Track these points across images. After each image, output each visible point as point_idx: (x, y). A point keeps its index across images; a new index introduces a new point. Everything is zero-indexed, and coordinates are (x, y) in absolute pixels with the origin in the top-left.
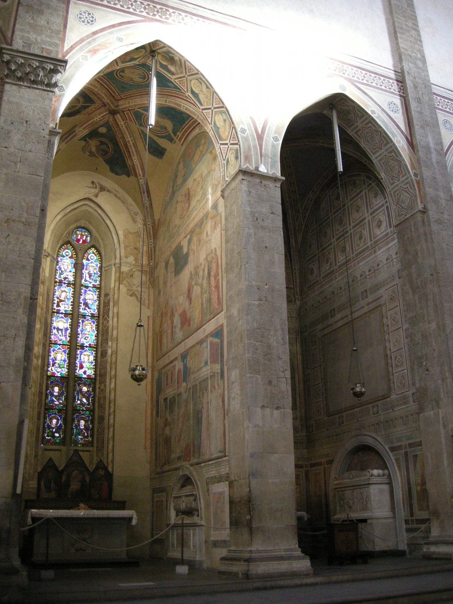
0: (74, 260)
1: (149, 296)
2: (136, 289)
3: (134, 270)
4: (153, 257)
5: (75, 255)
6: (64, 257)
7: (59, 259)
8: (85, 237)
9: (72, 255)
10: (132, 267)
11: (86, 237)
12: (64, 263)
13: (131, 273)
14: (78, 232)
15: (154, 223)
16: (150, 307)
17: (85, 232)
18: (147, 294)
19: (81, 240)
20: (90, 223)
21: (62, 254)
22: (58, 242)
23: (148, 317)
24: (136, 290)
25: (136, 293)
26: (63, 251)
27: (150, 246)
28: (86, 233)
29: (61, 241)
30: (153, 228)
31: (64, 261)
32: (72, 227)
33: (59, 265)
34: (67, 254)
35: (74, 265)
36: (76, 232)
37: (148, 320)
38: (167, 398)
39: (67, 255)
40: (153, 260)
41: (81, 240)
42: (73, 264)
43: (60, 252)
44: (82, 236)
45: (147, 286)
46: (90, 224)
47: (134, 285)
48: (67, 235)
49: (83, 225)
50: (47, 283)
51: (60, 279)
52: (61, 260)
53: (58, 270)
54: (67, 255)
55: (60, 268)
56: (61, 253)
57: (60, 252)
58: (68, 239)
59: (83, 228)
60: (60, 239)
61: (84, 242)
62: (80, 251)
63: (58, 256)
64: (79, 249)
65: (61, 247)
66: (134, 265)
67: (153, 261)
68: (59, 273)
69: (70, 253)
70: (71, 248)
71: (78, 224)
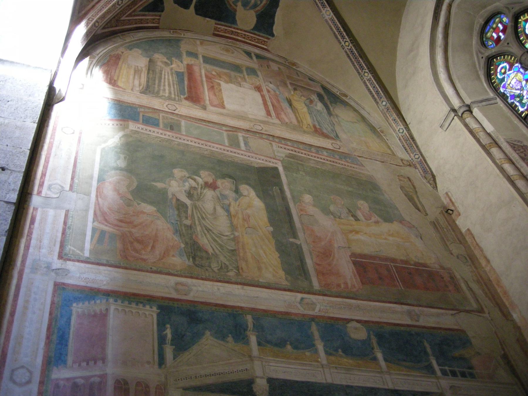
0: (517, 63)
5: (511, 58)
6: (503, 79)
7: (502, 90)
8: (500, 26)
9: (509, 63)
11: (501, 22)
12: (511, 85)
14: (489, 35)
17: (494, 22)
19: (501, 34)
20: (484, 7)
21: (499, 79)
22: (478, 78)
26: (496, 75)
28: (497, 20)
29: (479, 72)
31: (508, 83)
32: (475, 40)
33: (508, 95)
34: (503, 71)
35: (522, 67)
36: (487, 38)
39: (505, 73)
41: (501, 34)
42: (521, 70)
43: (495, 82)
44: (496, 30)
46: (485, 7)
48: (480, 56)
49: (482, 21)
50: (500, 137)
51: (526, 108)
52: (504, 87)
53: (513, 103)
54: (505, 73)
55: (513, 97)
56: (497, 81)
57: (495, 82)
58: (484, 58)
59: (487, 22)
60: (477, 72)
61: (504, 31)
62: (510, 45)
63: (496, 89)
64: (506, 44)
65: (489, 76)
68: (518, 104)
69: (505, 64)
70: (500, 59)
71: (477, 28)
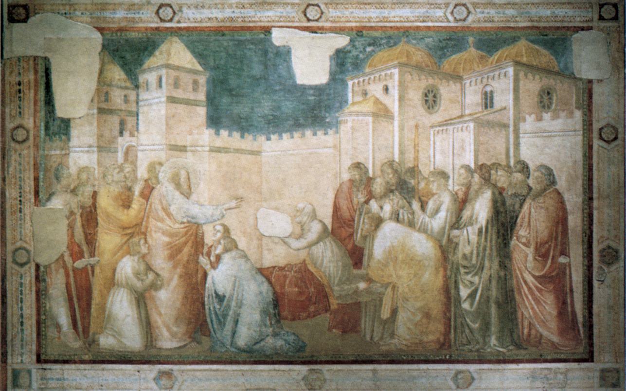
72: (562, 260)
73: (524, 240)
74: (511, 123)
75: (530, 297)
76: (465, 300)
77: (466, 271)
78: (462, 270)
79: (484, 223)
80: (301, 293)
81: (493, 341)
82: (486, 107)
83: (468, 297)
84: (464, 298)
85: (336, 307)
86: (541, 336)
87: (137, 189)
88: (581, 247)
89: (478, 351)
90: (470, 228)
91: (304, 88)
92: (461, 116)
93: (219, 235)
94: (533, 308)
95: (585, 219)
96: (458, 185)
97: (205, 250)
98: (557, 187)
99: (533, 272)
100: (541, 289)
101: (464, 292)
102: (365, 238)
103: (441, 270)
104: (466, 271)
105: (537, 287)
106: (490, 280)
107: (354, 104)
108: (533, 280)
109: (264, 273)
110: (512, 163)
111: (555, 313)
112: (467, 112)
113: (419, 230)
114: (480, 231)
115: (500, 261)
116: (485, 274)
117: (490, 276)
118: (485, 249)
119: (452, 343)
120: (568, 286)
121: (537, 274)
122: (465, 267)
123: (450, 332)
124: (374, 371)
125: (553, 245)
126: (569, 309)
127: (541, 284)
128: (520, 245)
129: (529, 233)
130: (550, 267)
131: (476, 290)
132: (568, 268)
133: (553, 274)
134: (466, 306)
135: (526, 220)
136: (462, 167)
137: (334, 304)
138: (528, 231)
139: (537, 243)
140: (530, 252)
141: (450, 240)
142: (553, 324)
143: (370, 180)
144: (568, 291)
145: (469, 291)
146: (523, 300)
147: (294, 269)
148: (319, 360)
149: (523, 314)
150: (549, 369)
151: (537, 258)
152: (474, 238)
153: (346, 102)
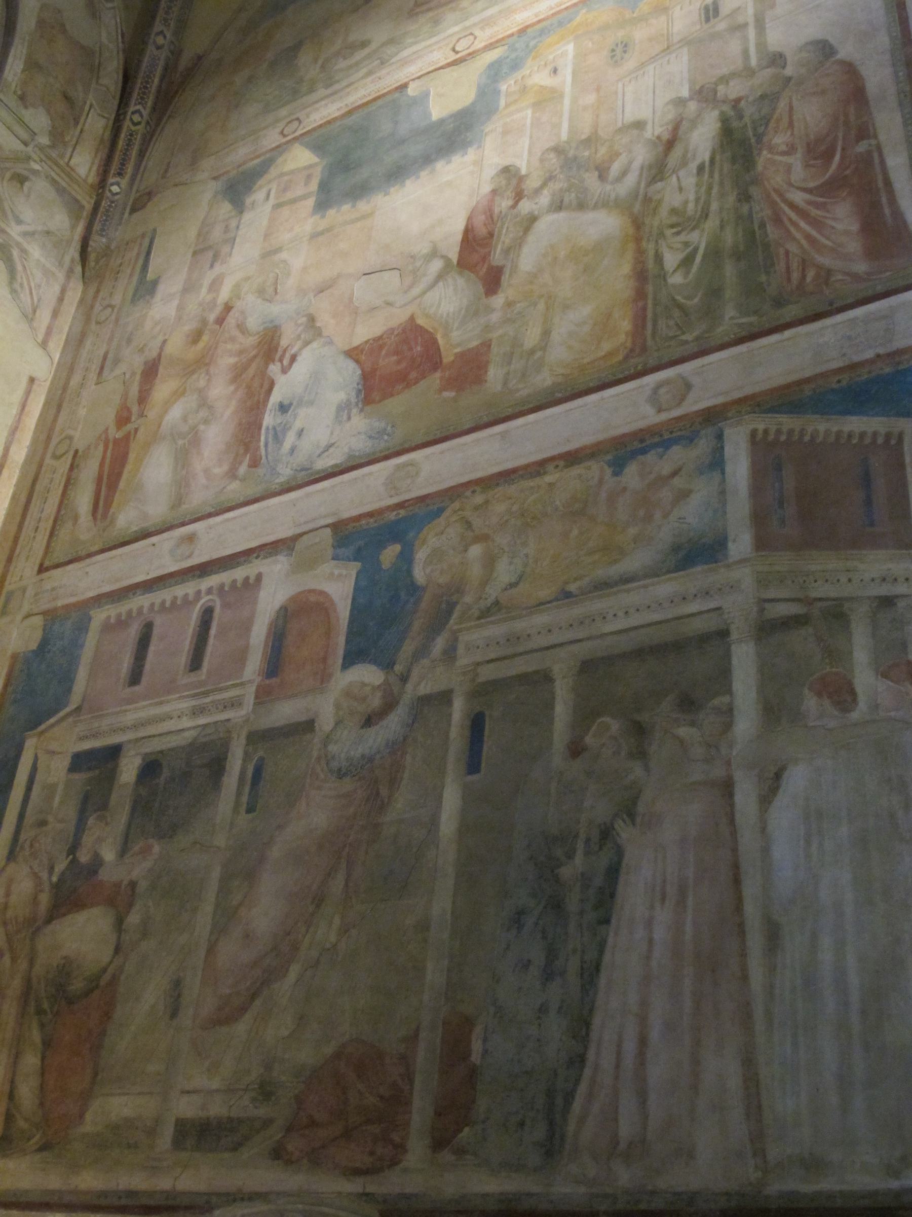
1: (61, 299)
2: (19, 239)
3: (36, 167)
4: (130, 169)
10: (29, 149)
13: (20, 169)
15: (177, 53)
16: (51, 345)
18: (57, 289)
23: (32, 380)
24: (18, 245)
25: (15, 253)
27: (127, 123)
30: (166, 69)
37: (28, 392)
38: (114, 753)
40: (128, 177)
45: (67, 259)
47: (19, 222)
66: (41, 148)
67: (124, 182)
72: (862, 147)
73: (783, 148)
74: (751, 20)
75: (802, 224)
76: (675, 271)
77: (675, 230)
78: (669, 232)
79: (707, 157)
80: (399, 362)
81: (730, 312)
82: (708, 20)
83: (679, 267)
84: (671, 271)
85: (452, 358)
86: (829, 272)
87: (212, 317)
88: (899, 114)
89: (697, 339)
90: (682, 173)
91: (442, 121)
92: (668, 48)
93: (301, 328)
94: (808, 237)
95: (901, 74)
96: (661, 126)
97: (277, 357)
98: (839, 57)
99: (803, 185)
100: (825, 203)
101: (671, 260)
102: (507, 251)
103: (631, 246)
104: (675, 230)
105: (810, 203)
106: (722, 227)
107: (507, 105)
108: (807, 196)
109: (353, 354)
110: (754, 62)
111: (855, 227)
112: (675, 40)
113: (595, 207)
114: (701, 169)
115: (739, 194)
116: (711, 224)
117: (722, 221)
118: (710, 188)
119: (650, 342)
120: (880, 178)
121: (812, 185)
122: (672, 226)
123: (644, 326)
124: (504, 435)
125: (840, 135)
126: (887, 211)
127: (821, 197)
128: (779, 158)
129: (792, 134)
130: (840, 165)
131: (696, 249)
132: (876, 155)
133: (848, 172)
134: (677, 279)
135: (786, 120)
136: (667, 104)
137: (448, 357)
138: (789, 133)
139: (808, 144)
140: (796, 161)
141: (647, 200)
142: (854, 246)
143: (521, 179)
144: (880, 184)
145: (681, 256)
146: (788, 231)
147: (396, 333)
148: (413, 445)
149: (787, 253)
150: (853, 320)
151: (812, 162)
152: (689, 179)
153: (497, 109)
